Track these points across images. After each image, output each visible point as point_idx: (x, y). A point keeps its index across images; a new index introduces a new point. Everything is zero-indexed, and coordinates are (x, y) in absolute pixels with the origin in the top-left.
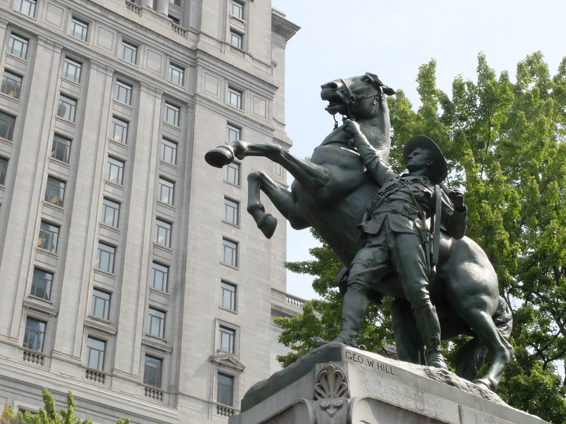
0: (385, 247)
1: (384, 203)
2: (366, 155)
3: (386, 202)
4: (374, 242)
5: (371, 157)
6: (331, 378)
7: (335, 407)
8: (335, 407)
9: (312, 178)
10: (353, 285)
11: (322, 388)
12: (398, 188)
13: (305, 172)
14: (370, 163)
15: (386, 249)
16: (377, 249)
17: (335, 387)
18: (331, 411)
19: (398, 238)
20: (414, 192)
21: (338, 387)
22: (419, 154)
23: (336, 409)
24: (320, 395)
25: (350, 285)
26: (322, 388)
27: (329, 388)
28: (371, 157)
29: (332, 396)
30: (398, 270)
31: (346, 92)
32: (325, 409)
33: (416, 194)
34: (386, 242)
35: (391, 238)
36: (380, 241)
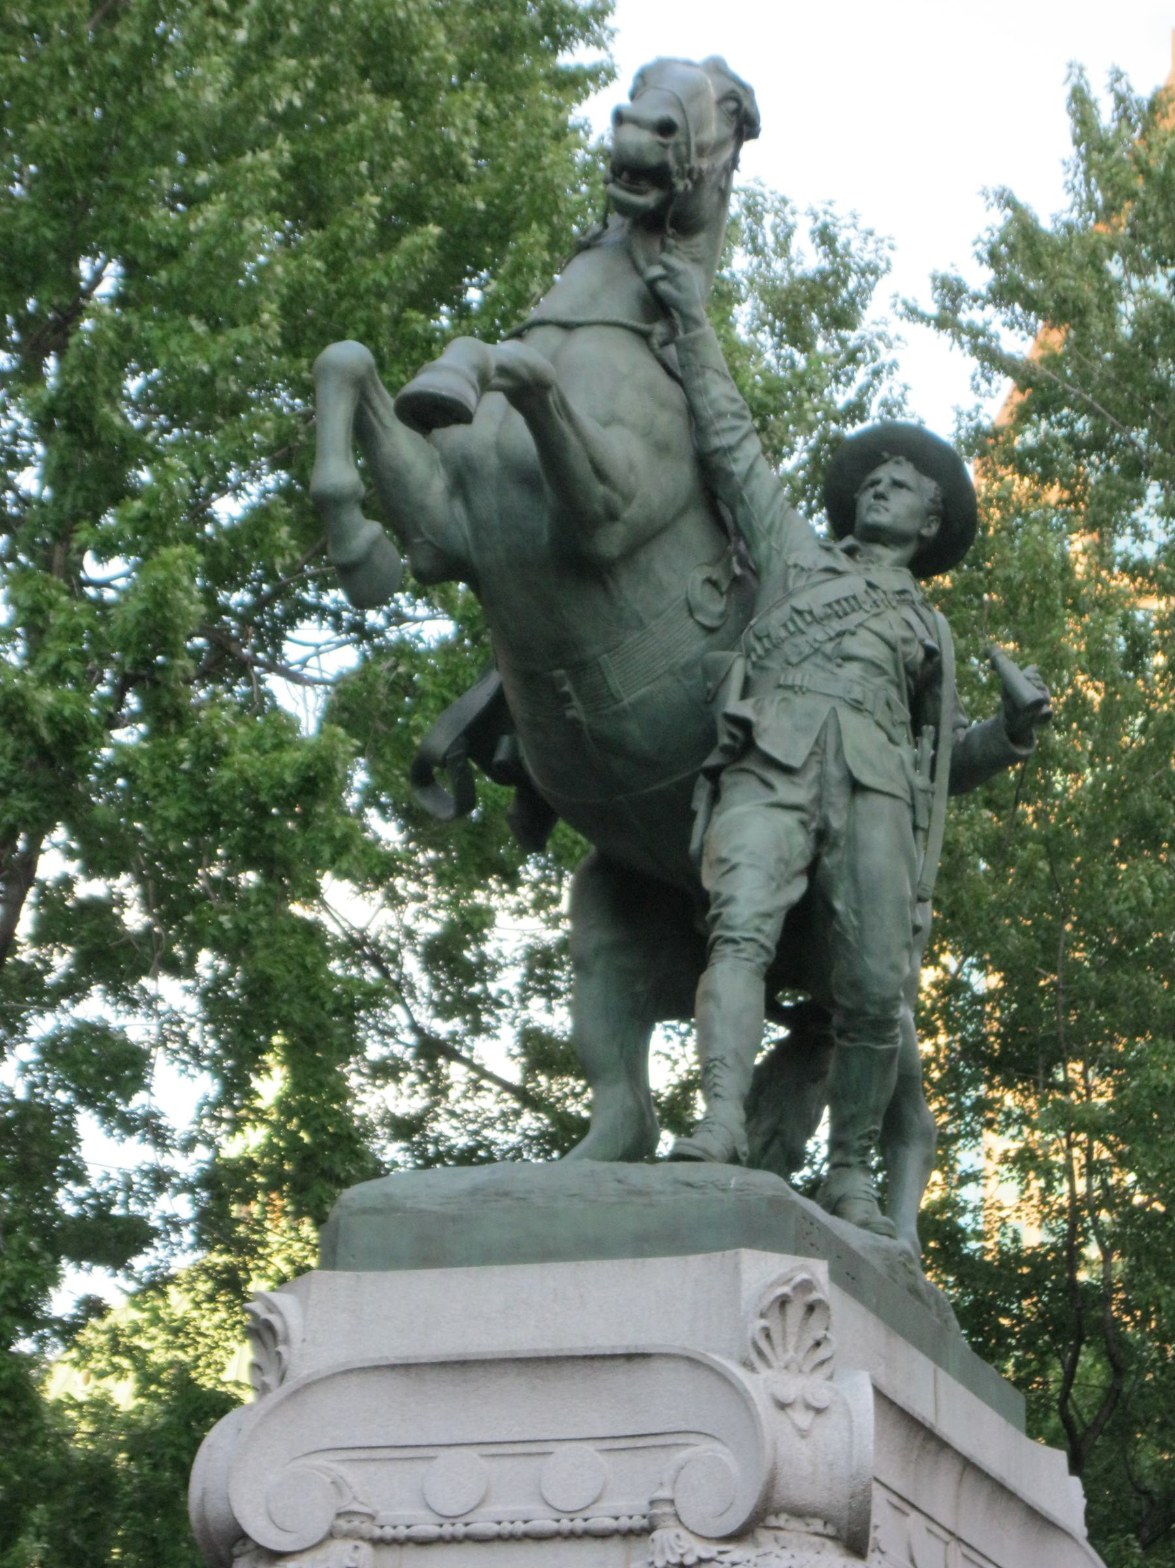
0: (813, 816)
1: (819, 660)
2: (720, 415)
3: (828, 658)
4: (787, 791)
5: (733, 429)
6: (795, 1312)
7: (808, 1407)
8: (808, 1407)
9: (601, 489)
10: (743, 945)
11: (768, 1336)
12: (864, 616)
13: (588, 467)
14: (730, 449)
15: (814, 825)
16: (790, 819)
17: (800, 1338)
19: (861, 802)
20: (905, 641)
21: (811, 1342)
22: (909, 489)
23: (811, 1414)
24: (760, 1353)
25: (733, 941)
26: (768, 1336)
27: (784, 1338)
28: (733, 429)
29: (794, 1367)
30: (839, 905)
31: (683, 149)
32: (782, 1406)
33: (907, 649)
34: (818, 800)
35: (838, 796)
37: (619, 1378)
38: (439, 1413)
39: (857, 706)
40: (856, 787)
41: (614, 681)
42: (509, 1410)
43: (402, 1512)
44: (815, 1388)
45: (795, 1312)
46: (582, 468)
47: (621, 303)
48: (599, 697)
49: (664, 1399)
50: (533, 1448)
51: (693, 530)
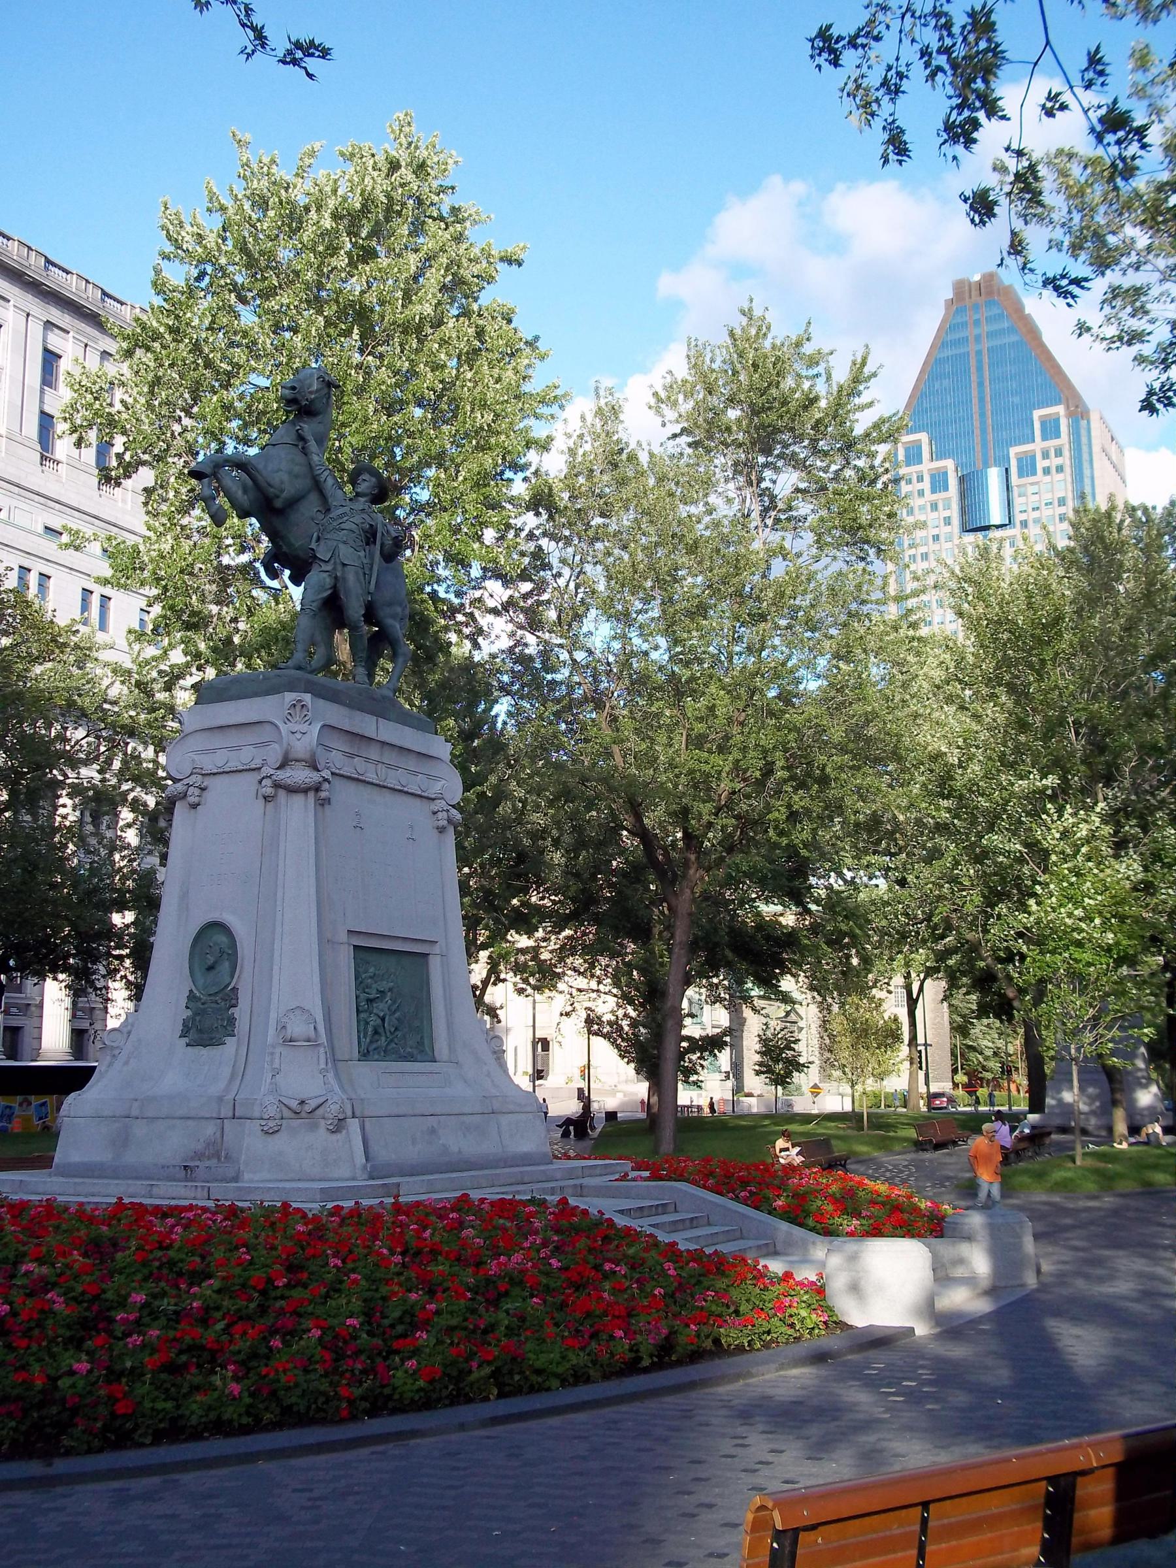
4: (324, 567)
6: (298, 708)
18: (298, 736)
35: (339, 567)
36: (329, 567)
37: (257, 728)
38: (217, 741)
39: (345, 543)
40: (344, 565)
41: (292, 540)
42: (233, 738)
43: (209, 767)
44: (304, 727)
45: (298, 708)
46: (264, 485)
47: (291, 438)
48: (290, 545)
49: (266, 733)
50: (238, 748)
51: (314, 497)
